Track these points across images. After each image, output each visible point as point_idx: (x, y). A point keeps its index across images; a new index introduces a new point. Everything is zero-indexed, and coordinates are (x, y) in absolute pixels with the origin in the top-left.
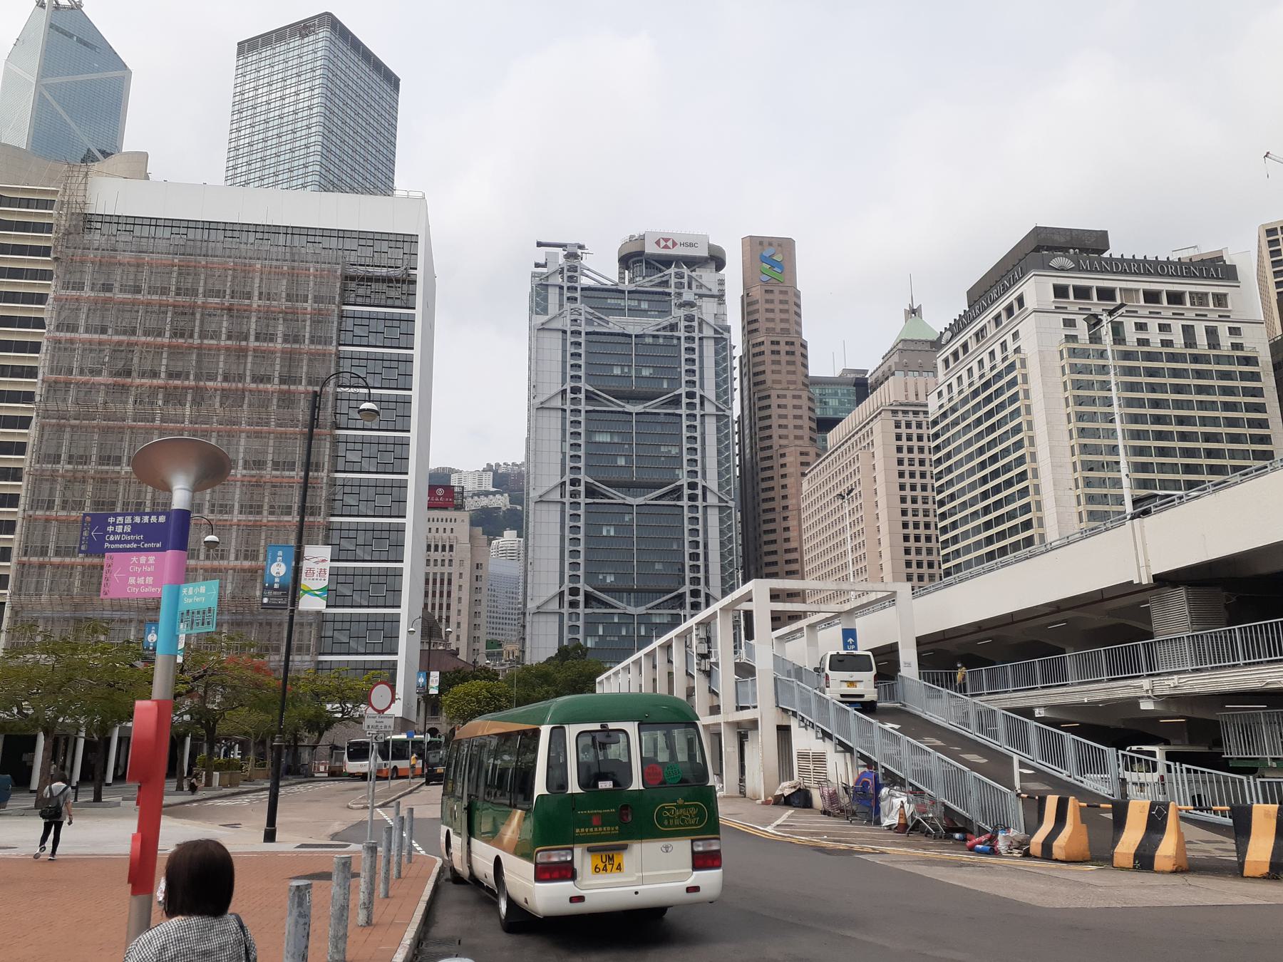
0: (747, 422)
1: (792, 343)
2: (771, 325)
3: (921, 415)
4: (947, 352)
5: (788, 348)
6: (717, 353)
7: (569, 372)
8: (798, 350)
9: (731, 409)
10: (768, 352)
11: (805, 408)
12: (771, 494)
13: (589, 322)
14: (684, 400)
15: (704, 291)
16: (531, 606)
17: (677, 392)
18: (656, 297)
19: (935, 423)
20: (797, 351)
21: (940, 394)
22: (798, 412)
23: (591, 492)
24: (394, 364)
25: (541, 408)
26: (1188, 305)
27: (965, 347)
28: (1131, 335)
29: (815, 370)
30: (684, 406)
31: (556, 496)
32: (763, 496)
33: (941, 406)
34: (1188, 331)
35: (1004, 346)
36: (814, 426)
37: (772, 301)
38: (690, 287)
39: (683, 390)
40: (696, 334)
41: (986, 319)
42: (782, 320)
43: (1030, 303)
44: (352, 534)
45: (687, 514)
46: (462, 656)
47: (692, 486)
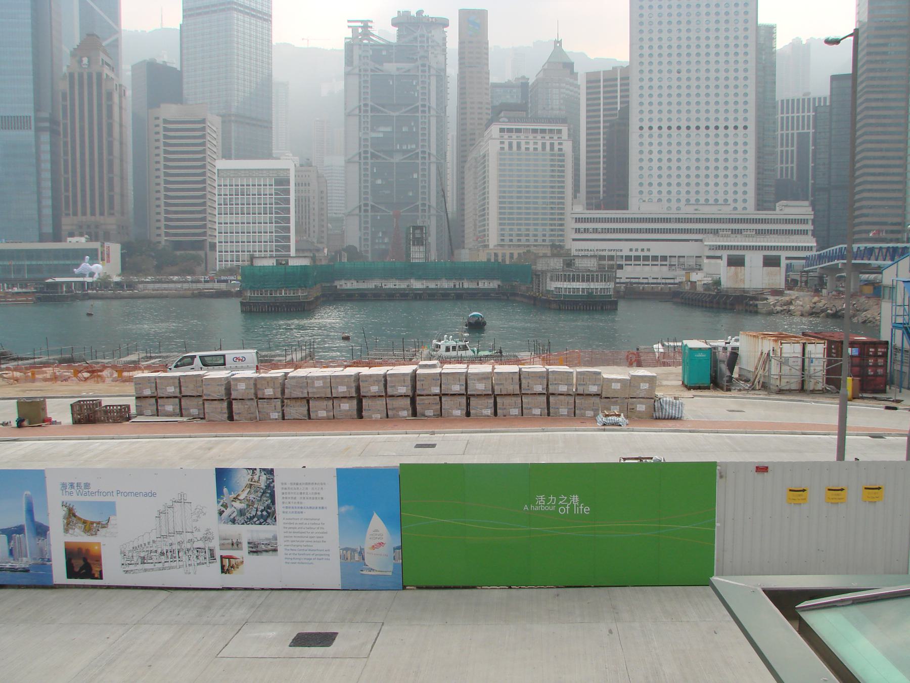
6: (437, 81)
23: (373, 156)
28: (523, 147)
34: (544, 145)
39: (420, 103)
40: (427, 74)
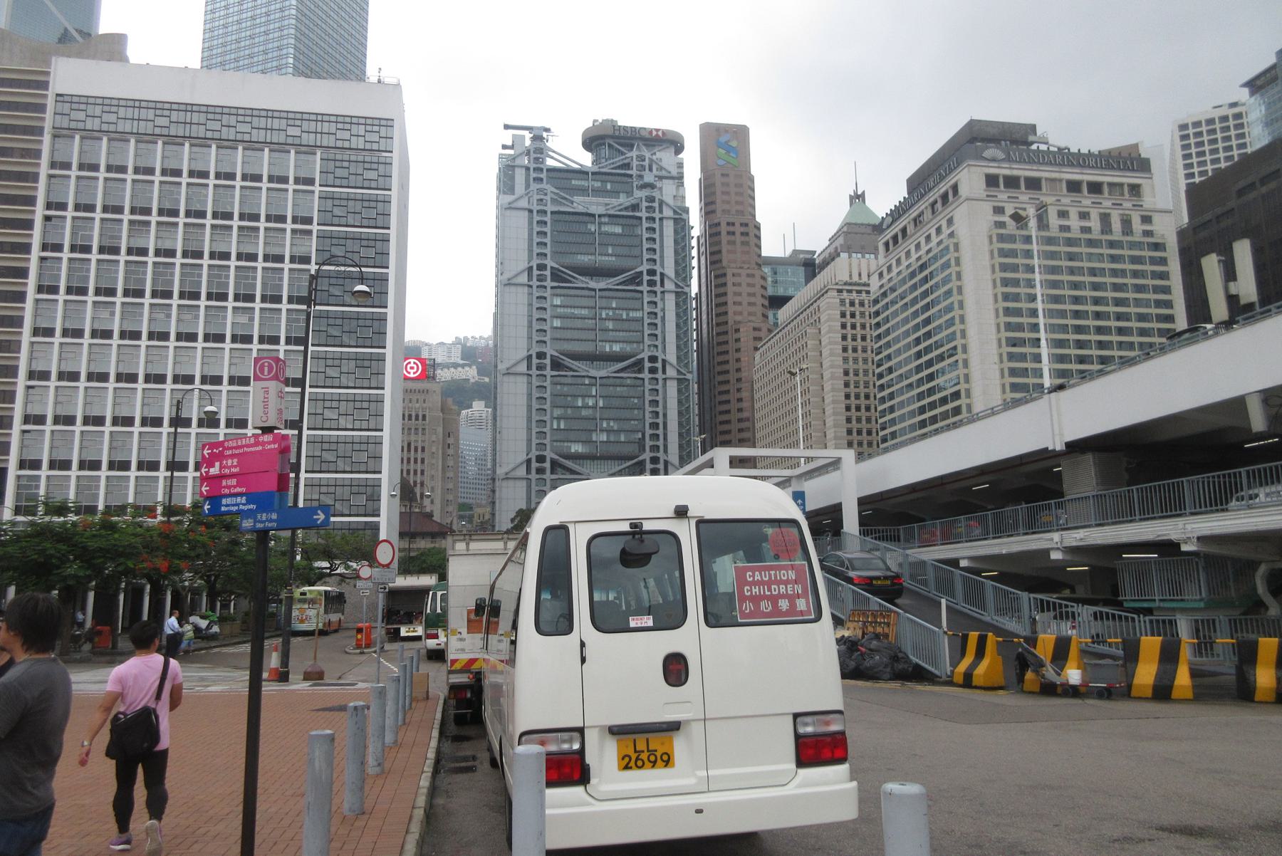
0: (704, 299)
1: (746, 225)
2: (726, 207)
3: (864, 294)
4: (888, 235)
5: (743, 229)
7: (536, 250)
8: (752, 232)
9: (689, 286)
10: (724, 233)
11: (758, 286)
12: (725, 367)
13: (553, 200)
14: (646, 278)
15: (664, 173)
16: (500, 471)
17: (638, 270)
18: (619, 178)
19: (876, 301)
20: (751, 232)
21: (881, 275)
22: (751, 290)
23: (556, 365)
24: (372, 243)
25: (509, 284)
26: (1106, 194)
27: (904, 230)
28: (1054, 221)
29: (766, 252)
30: (645, 283)
31: (523, 368)
32: (719, 369)
33: (882, 286)
34: (1105, 218)
35: (939, 231)
36: (766, 303)
37: (728, 185)
38: (651, 170)
39: (644, 268)
40: (657, 215)
41: (923, 205)
42: (737, 203)
43: (964, 191)
44: (335, 404)
45: (648, 386)
46: (437, 518)
47: (653, 359)
